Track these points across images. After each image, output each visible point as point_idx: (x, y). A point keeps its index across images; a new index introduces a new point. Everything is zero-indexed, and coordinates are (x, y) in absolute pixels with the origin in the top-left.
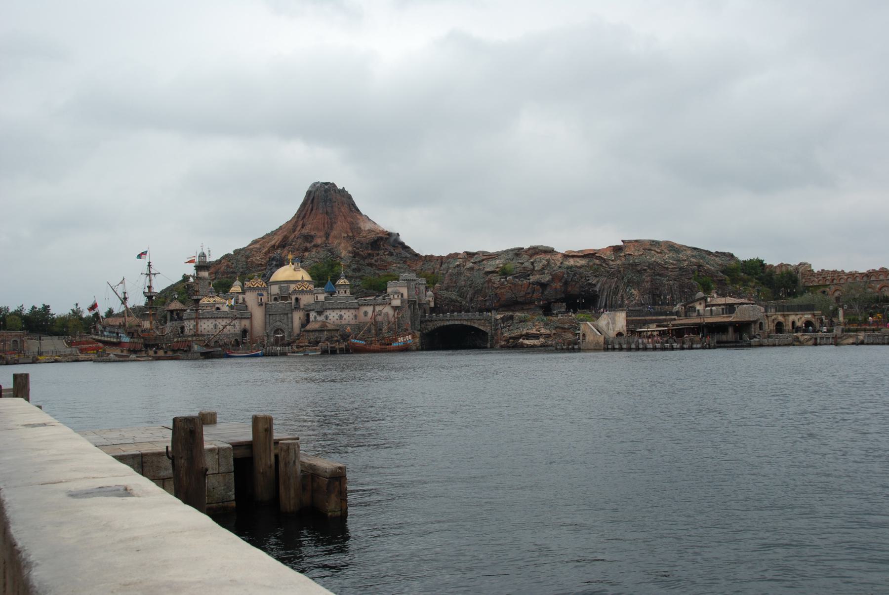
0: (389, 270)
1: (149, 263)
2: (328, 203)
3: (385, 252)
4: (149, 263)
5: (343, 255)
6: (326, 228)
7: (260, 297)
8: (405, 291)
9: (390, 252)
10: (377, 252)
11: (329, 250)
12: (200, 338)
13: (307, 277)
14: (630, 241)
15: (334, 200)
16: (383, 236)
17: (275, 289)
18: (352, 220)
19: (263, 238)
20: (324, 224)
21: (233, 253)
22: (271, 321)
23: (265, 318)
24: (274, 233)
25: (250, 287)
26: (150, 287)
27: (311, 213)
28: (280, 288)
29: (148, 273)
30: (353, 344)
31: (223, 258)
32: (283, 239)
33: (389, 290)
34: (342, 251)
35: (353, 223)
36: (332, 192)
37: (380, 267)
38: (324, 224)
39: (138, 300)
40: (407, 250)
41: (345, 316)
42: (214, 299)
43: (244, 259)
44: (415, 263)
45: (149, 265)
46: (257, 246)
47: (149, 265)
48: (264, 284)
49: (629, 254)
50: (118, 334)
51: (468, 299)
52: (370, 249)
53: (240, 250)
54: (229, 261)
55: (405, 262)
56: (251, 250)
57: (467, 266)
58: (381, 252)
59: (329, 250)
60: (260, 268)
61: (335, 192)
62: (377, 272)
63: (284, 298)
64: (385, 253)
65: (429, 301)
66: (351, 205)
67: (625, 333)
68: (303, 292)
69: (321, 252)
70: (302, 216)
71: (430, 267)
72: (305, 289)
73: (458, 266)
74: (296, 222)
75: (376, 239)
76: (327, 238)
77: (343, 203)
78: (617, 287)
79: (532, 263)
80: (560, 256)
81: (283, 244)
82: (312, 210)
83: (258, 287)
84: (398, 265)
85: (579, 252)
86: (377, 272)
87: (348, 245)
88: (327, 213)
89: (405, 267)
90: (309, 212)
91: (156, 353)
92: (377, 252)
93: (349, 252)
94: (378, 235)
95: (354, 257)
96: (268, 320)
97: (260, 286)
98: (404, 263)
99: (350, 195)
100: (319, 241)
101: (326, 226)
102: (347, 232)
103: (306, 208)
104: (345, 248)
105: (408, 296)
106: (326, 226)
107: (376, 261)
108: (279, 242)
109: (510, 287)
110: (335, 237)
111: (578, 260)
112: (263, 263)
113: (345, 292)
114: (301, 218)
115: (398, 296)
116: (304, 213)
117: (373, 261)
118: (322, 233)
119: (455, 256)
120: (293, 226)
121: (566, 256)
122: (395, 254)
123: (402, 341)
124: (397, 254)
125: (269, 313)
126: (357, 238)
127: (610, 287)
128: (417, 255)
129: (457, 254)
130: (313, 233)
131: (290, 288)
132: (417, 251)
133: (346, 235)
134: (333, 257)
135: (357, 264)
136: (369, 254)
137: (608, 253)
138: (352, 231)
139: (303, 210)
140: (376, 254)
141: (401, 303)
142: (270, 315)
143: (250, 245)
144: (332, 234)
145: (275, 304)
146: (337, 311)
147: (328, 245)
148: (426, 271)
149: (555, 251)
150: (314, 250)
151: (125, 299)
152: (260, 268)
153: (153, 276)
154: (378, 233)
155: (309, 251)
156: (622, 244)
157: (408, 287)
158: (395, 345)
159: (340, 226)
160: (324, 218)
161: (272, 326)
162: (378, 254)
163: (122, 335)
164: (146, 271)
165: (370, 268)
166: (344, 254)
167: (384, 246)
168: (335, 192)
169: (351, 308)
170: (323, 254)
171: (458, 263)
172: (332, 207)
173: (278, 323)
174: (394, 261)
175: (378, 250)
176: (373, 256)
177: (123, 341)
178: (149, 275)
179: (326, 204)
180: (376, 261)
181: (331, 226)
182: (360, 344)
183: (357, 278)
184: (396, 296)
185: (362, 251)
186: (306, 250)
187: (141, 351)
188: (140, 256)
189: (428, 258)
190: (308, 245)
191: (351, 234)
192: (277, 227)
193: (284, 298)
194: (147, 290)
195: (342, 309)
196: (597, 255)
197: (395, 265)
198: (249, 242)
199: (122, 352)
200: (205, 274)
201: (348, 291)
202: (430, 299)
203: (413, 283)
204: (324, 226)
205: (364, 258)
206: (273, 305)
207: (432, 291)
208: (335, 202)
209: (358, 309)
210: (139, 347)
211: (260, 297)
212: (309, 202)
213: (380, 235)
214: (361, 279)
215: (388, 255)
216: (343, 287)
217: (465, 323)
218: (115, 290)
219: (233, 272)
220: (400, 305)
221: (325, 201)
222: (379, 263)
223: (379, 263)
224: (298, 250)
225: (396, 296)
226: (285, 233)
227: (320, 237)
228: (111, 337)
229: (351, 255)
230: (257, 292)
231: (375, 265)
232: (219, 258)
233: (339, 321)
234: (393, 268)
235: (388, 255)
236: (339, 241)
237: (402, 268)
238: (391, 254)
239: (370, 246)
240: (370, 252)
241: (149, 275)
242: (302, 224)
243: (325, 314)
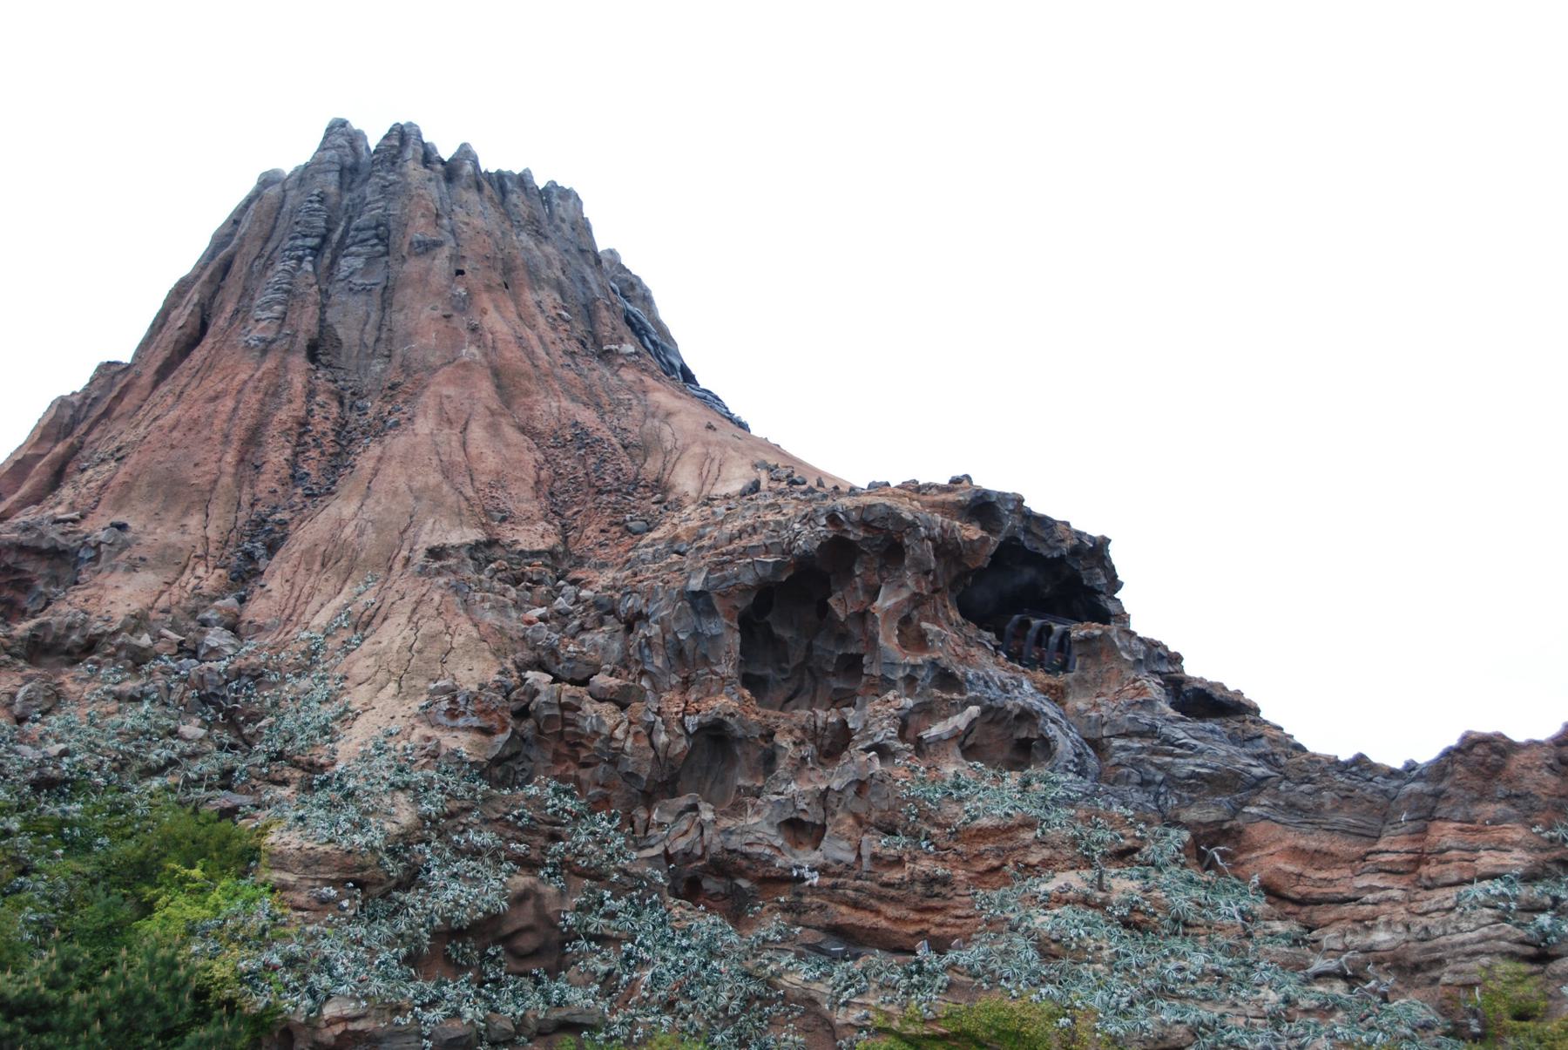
0: (968, 956)
3: (928, 711)
5: (349, 747)
10: (827, 716)
20: (254, 438)
34: (357, 697)
35: (583, 439)
37: (845, 915)
38: (254, 438)
44: (1394, 846)
52: (727, 669)
62: (797, 976)
75: (807, 538)
76: (244, 576)
84: (1123, 885)
86: (797, 976)
92: (827, 716)
101: (276, 455)
106: (276, 455)
107: (799, 830)
122: (1065, 743)
124: (1097, 745)
134: (226, 779)
135: (528, 864)
138: (555, 512)
140: (812, 734)
144: (309, 533)
160: (275, 392)
162: (834, 744)
165: (706, 922)
167: (915, 639)
172: (387, 296)
175: (844, 699)
176: (769, 760)
180: (799, 830)
185: (621, 700)
204: (249, 463)
208: (427, 248)
222: (836, 849)
223: (836, 849)
229: (461, 743)
231: (788, 880)
234: (1042, 921)
236: (369, 597)
237: (1182, 925)
239: (734, 640)
240: (723, 703)
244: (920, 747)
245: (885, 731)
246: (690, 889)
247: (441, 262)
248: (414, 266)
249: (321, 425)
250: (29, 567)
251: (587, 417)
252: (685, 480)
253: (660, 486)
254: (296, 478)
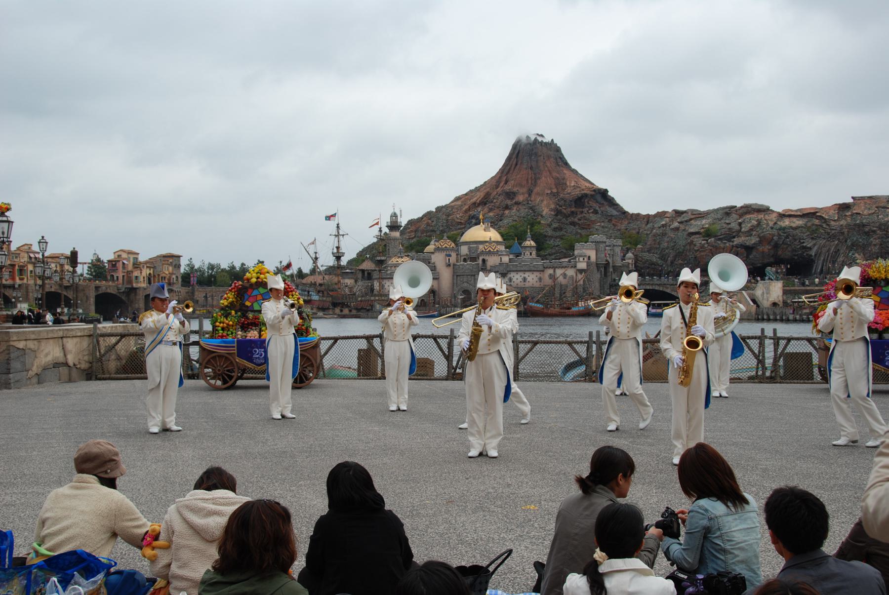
0: (591, 230)
1: (338, 224)
2: (533, 157)
3: (589, 210)
4: (338, 224)
5: (544, 213)
6: (530, 184)
7: (448, 258)
8: (593, 254)
9: (594, 209)
11: (531, 208)
12: (383, 298)
13: (499, 238)
14: (862, 198)
15: (540, 153)
16: (588, 192)
17: (464, 250)
18: (558, 175)
19: (466, 194)
20: (527, 180)
21: (434, 210)
22: (459, 282)
23: (453, 279)
24: (477, 189)
25: (438, 247)
26: (338, 248)
27: (515, 168)
28: (470, 249)
29: (337, 234)
30: (531, 307)
31: (424, 215)
32: (484, 196)
33: (576, 252)
35: (558, 178)
36: (538, 145)
39: (327, 260)
40: (615, 207)
41: (529, 279)
43: (444, 217)
44: (620, 222)
45: (338, 227)
46: (459, 203)
47: (338, 227)
48: (453, 245)
49: (857, 213)
50: (309, 292)
51: (669, 262)
52: (573, 206)
53: (442, 207)
54: (430, 219)
55: (610, 221)
56: (452, 207)
57: (672, 227)
58: (585, 210)
59: (531, 208)
60: (459, 227)
61: (541, 145)
62: (579, 231)
63: (474, 259)
64: (590, 211)
65: (629, 263)
66: (559, 160)
67: (781, 304)
68: (490, 253)
69: (522, 210)
70: (506, 171)
71: (634, 226)
72: (492, 250)
73: (663, 226)
74: (500, 178)
75: (580, 196)
76: (530, 195)
77: (549, 157)
78: (837, 252)
79: (740, 224)
80: (774, 215)
81: (483, 202)
82: (516, 164)
83: (446, 247)
84: (603, 224)
85: (796, 211)
86: (579, 231)
87: (551, 202)
88: (531, 168)
89: (609, 226)
90: (513, 166)
91: (341, 311)
93: (551, 210)
94: (583, 192)
95: (556, 215)
96: (455, 281)
98: (609, 221)
99: (559, 147)
100: (520, 198)
101: (530, 181)
102: (551, 189)
103: (511, 163)
104: (548, 206)
105: (596, 259)
106: (530, 181)
107: (579, 220)
108: (480, 199)
109: (711, 250)
110: (538, 194)
111: (795, 220)
112: (462, 221)
113: (531, 254)
114: (505, 173)
115: (584, 259)
116: (508, 168)
117: (576, 220)
118: (525, 190)
119: (661, 215)
120: (497, 182)
121: (782, 216)
122: (600, 212)
123: (583, 305)
125: (456, 275)
126: (562, 195)
127: (829, 250)
128: (625, 213)
129: (664, 213)
130: (515, 190)
131: (479, 248)
132: (626, 209)
133: (549, 192)
134: (534, 216)
136: (572, 212)
137: (832, 212)
138: (556, 187)
139: (507, 165)
141: (587, 266)
142: (457, 276)
143: (452, 202)
145: (463, 265)
146: (521, 274)
147: (530, 202)
148: (631, 231)
149: (771, 210)
150: (515, 208)
151: (316, 258)
152: (459, 227)
153: (341, 237)
154: (583, 190)
155: (510, 209)
156: (852, 201)
157: (596, 251)
158: (574, 309)
159: (545, 182)
161: (459, 287)
162: (582, 212)
163: (312, 294)
164: (335, 232)
165: (572, 227)
166: (546, 211)
168: (541, 145)
169: (535, 271)
170: (524, 211)
171: (663, 223)
172: (537, 162)
173: (466, 284)
174: (599, 220)
175: (583, 208)
177: (313, 299)
178: (337, 236)
179: (530, 158)
180: (579, 220)
181: (535, 182)
182: (538, 307)
183: (556, 237)
184: (581, 259)
185: (565, 209)
186: (507, 207)
187: (328, 309)
188: (328, 218)
189: (634, 216)
190: (509, 202)
191: (555, 191)
192: (482, 183)
193: (474, 259)
194: (335, 251)
195: (526, 271)
196: (817, 214)
197: (599, 224)
198: (452, 199)
200: (397, 234)
201: (534, 253)
202: (630, 261)
203: (602, 246)
205: (566, 216)
207: (633, 253)
208: (541, 156)
209: (543, 271)
210: (327, 305)
211: (448, 258)
212: (514, 156)
213: (585, 192)
214: (562, 239)
215: (593, 213)
216: (528, 249)
217: (657, 288)
218: (308, 250)
219: (433, 231)
220: (586, 268)
221: (530, 156)
222: (582, 221)
223: (582, 221)
224: (498, 208)
225: (581, 259)
226: (488, 190)
227: (523, 194)
229: (553, 213)
230: (445, 253)
231: (579, 224)
233: (523, 283)
235: (593, 213)
237: (606, 227)
238: (596, 212)
239: (574, 204)
240: (573, 209)
241: (337, 236)
242: (506, 180)
243: (509, 276)
244: (589, 213)
245: (586, 212)
246: (571, 224)
247: (542, 157)
248: (539, 158)
249: (533, 178)
251: (558, 175)
252: (568, 184)
253: (566, 184)
254: (532, 184)
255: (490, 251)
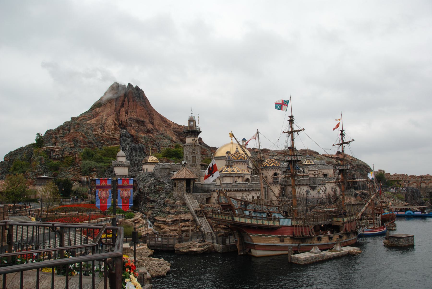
1: (291, 117)
4: (291, 117)
29: (290, 130)
42: (232, 169)
45: (291, 121)
47: (291, 121)
60: (114, 142)
97: (236, 159)
101: (147, 115)
106: (147, 115)
112: (116, 138)
152: (114, 142)
199: (282, 240)
204: (147, 116)
206: (255, 179)
221: (139, 97)
228: (256, 218)
232: (56, 128)
233: (317, 195)
241: (291, 133)
250: (140, 122)
254: (149, 117)
255: (273, 166)
